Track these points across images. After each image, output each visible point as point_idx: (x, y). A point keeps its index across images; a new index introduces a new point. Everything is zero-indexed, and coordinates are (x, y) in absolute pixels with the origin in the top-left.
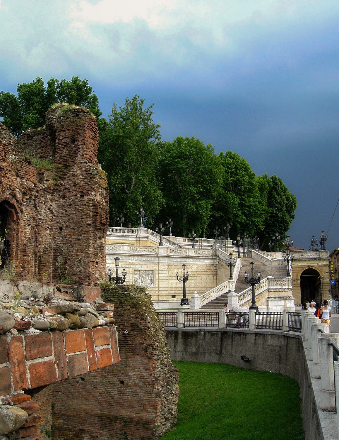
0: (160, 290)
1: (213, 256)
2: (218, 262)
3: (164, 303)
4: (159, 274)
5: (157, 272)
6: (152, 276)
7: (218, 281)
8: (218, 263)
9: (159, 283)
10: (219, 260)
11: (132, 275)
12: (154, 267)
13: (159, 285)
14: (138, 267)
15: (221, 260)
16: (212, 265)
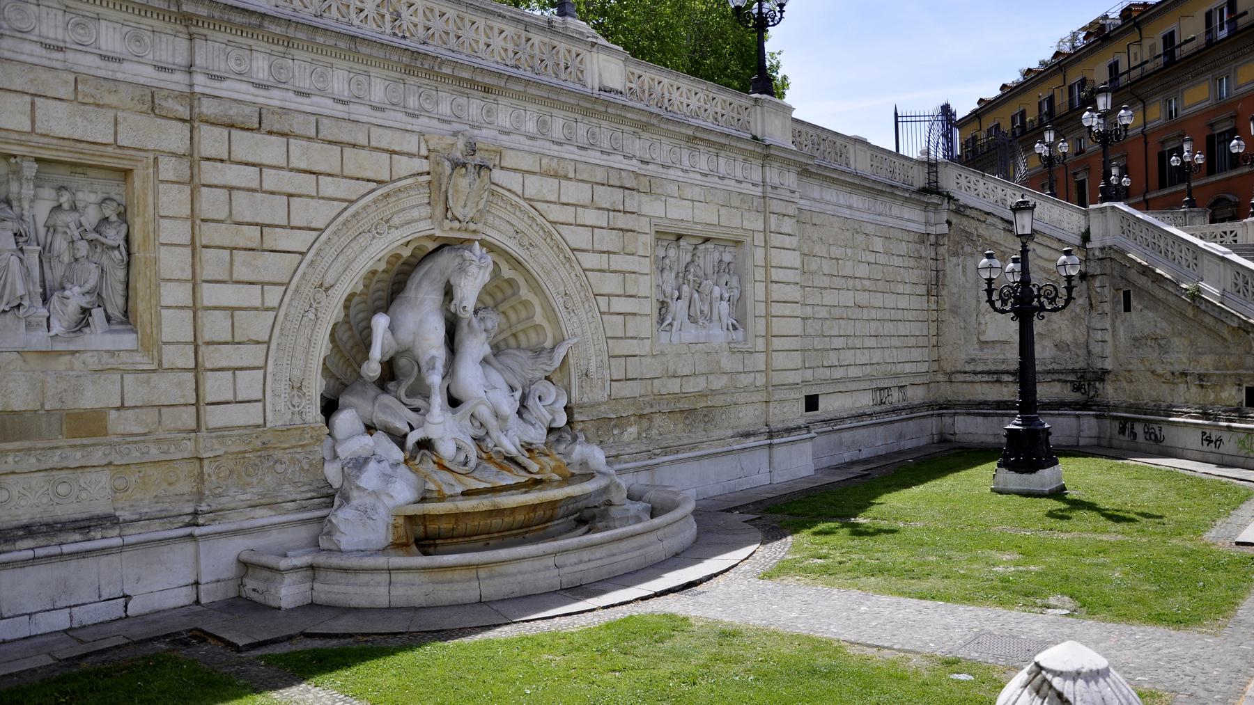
0: (775, 365)
1: (924, 191)
2: (949, 223)
3: (794, 447)
4: (767, 266)
5: (759, 253)
6: (734, 282)
7: (946, 316)
8: (945, 229)
9: (767, 326)
10: (957, 212)
11: (646, 266)
12: (746, 225)
13: (768, 336)
14: (678, 212)
15: (968, 212)
16: (923, 238)
